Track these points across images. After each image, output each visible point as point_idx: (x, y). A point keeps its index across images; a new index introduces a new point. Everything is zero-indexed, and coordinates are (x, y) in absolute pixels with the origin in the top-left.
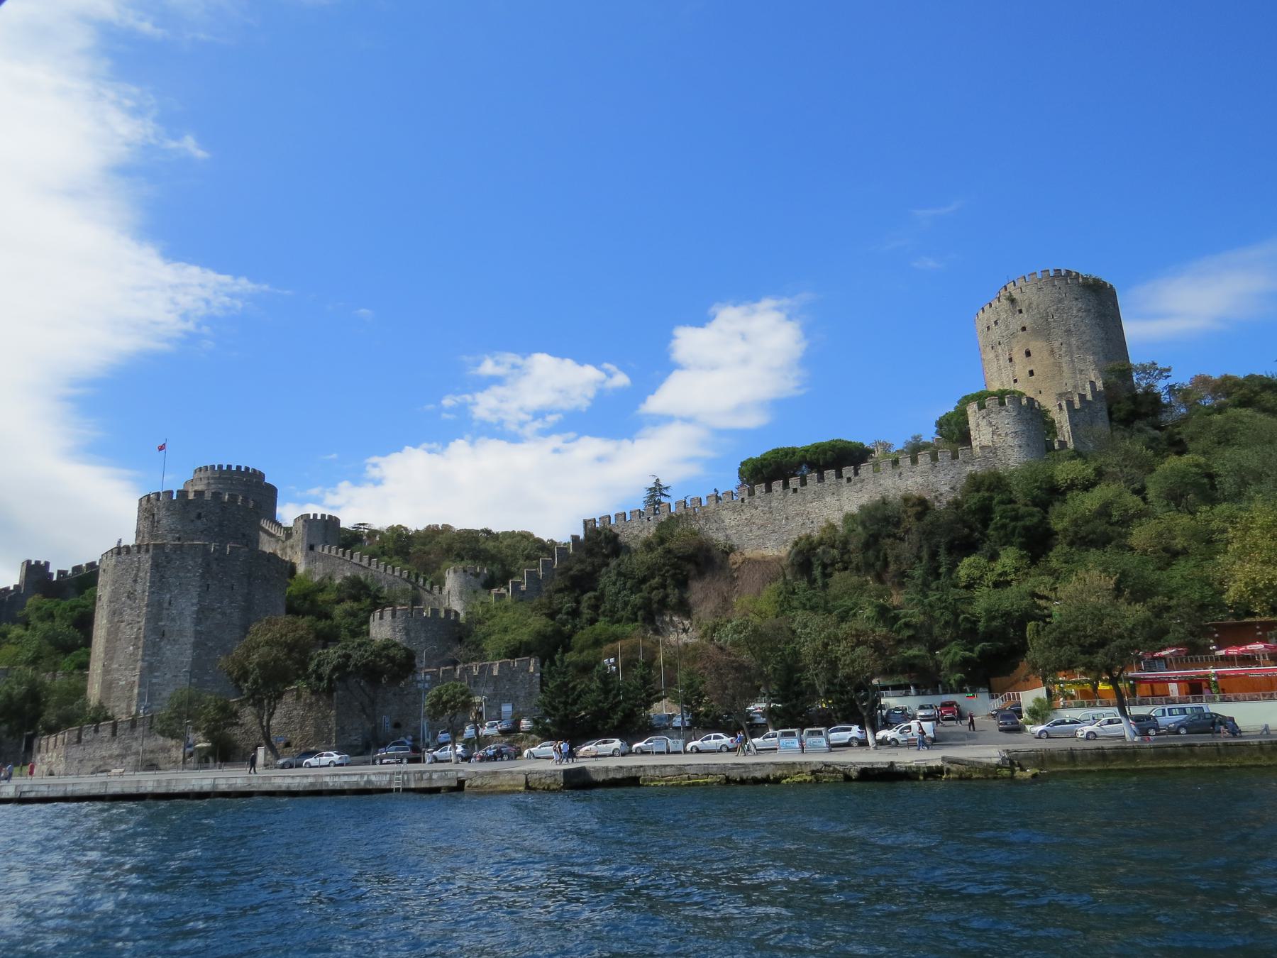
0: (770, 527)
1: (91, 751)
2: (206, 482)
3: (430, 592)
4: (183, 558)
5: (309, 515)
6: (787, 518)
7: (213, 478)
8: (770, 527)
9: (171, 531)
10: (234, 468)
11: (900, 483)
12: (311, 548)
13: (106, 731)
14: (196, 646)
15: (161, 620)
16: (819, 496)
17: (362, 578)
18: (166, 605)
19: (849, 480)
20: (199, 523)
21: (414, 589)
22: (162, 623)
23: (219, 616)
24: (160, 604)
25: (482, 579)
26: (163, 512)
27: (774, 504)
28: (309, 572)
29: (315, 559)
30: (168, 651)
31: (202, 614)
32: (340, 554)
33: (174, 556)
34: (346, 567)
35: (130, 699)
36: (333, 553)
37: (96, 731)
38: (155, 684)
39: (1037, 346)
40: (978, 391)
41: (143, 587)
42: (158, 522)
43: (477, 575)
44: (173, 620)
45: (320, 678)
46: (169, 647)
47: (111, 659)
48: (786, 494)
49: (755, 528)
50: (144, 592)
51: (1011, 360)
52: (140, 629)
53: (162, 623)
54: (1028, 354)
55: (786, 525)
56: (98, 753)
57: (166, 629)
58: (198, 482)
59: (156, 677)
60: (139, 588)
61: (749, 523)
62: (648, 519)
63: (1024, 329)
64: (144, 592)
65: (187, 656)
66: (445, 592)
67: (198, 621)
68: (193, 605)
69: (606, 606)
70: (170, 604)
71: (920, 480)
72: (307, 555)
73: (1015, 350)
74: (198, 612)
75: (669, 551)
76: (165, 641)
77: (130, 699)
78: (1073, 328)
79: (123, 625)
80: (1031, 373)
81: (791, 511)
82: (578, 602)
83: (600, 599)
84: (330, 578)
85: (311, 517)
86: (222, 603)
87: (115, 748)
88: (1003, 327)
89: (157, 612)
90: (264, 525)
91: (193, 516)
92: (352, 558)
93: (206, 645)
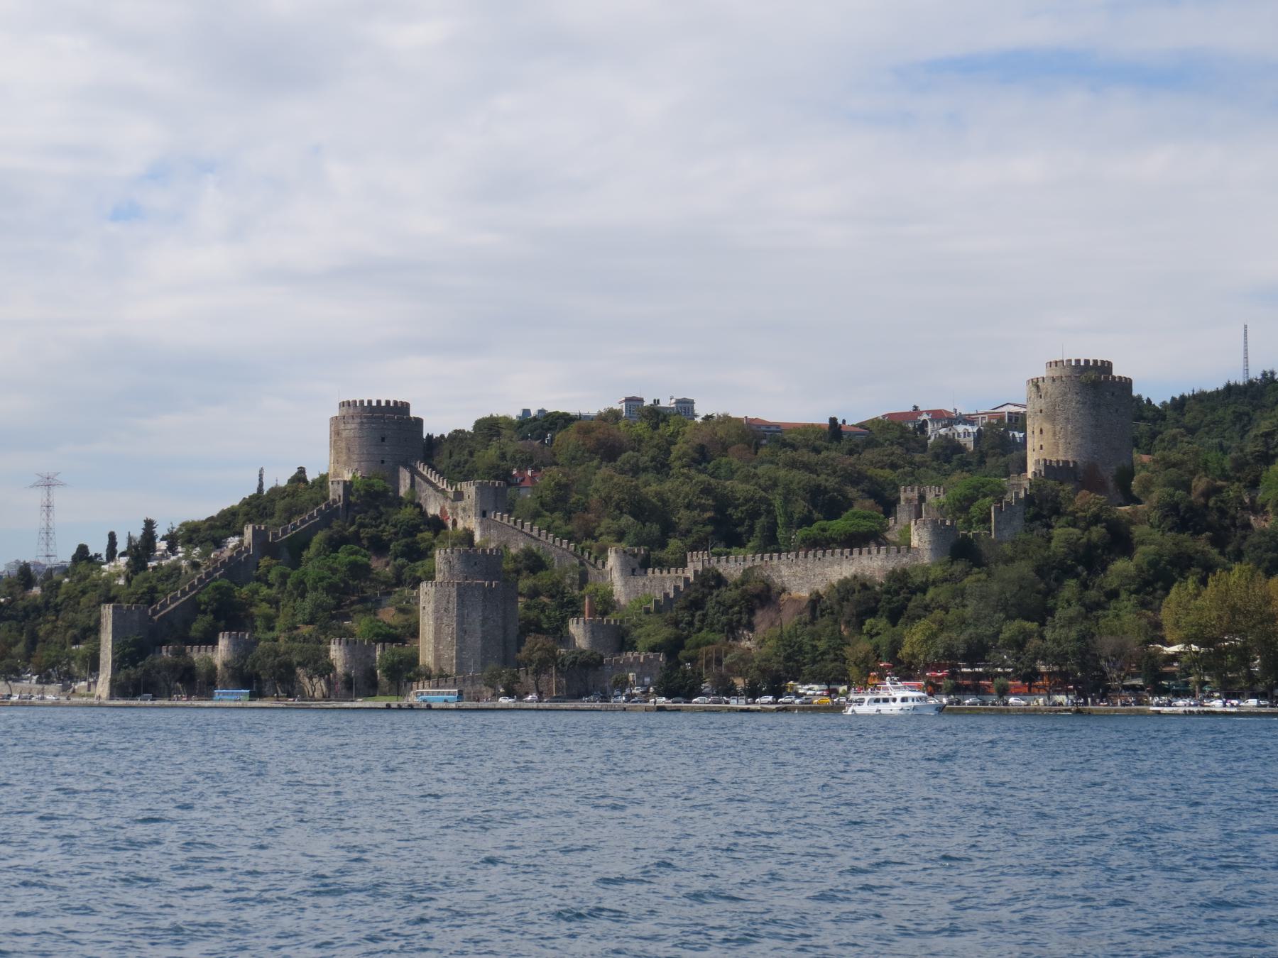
2: (359, 420)
3: (594, 566)
7: (366, 417)
9: (461, 572)
10: (383, 404)
12: (484, 514)
14: (483, 638)
16: (831, 564)
17: (535, 549)
21: (582, 564)
25: (639, 559)
26: (456, 561)
31: (485, 621)
32: (512, 523)
34: (520, 537)
35: (452, 665)
36: (505, 521)
41: (453, 606)
43: (635, 556)
45: (563, 666)
54: (1041, 431)
58: (350, 421)
60: (451, 606)
63: (1041, 411)
65: (479, 644)
67: (483, 625)
69: (708, 621)
71: (880, 563)
72: (481, 522)
75: (746, 591)
77: (452, 665)
81: (818, 570)
82: (693, 616)
83: (705, 615)
84: (505, 546)
89: (461, 619)
90: (421, 469)
91: (472, 564)
92: (523, 527)
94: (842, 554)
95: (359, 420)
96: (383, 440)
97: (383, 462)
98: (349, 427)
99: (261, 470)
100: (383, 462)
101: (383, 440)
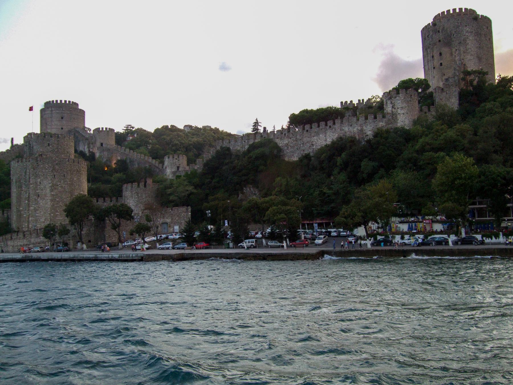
0: (296, 147)
1: (16, 243)
4: (44, 164)
5: (99, 128)
6: (303, 144)
8: (296, 147)
11: (351, 128)
13: (21, 235)
14: (52, 200)
15: (37, 190)
16: (317, 134)
18: (39, 183)
19: (330, 127)
20: (48, 148)
22: (38, 191)
23: (60, 188)
24: (36, 183)
27: (298, 137)
28: (100, 157)
29: (103, 151)
30: (41, 202)
31: (53, 187)
33: (40, 163)
37: (17, 235)
38: (37, 216)
39: (445, 50)
40: (408, 78)
42: (33, 147)
44: (42, 190)
46: (41, 201)
47: (20, 206)
48: (303, 133)
49: (290, 148)
50: (30, 178)
51: (433, 57)
52: (29, 194)
53: (38, 191)
55: (303, 147)
56: (19, 244)
57: (40, 194)
59: (38, 213)
61: (287, 145)
62: (245, 141)
63: (440, 41)
64: (30, 178)
65: (49, 204)
66: (164, 167)
67: (52, 191)
68: (50, 183)
70: (40, 183)
71: (359, 128)
73: (435, 52)
74: (51, 187)
76: (39, 198)
78: (462, 42)
79: (22, 192)
80: (441, 64)
85: (101, 129)
86: (60, 182)
87: (25, 242)
88: (431, 40)
91: (46, 145)
93: (56, 200)
94: (326, 125)
95: (50, 109)
96: (62, 118)
97: (62, 129)
98: (46, 113)
99: (12, 139)
100: (62, 129)
101: (62, 118)
